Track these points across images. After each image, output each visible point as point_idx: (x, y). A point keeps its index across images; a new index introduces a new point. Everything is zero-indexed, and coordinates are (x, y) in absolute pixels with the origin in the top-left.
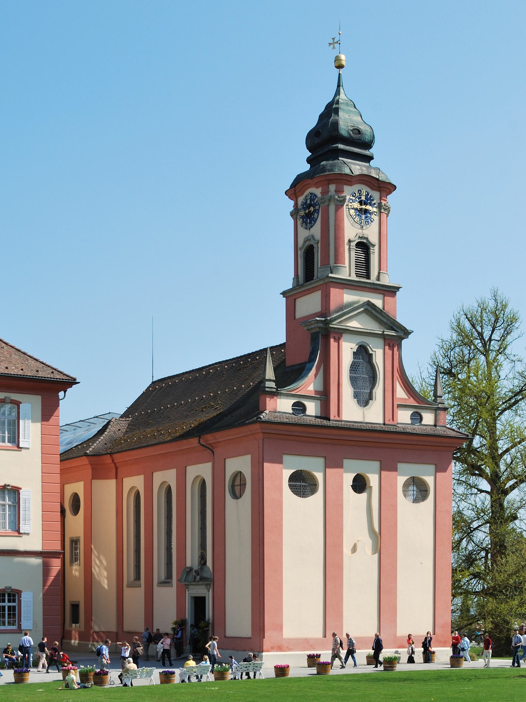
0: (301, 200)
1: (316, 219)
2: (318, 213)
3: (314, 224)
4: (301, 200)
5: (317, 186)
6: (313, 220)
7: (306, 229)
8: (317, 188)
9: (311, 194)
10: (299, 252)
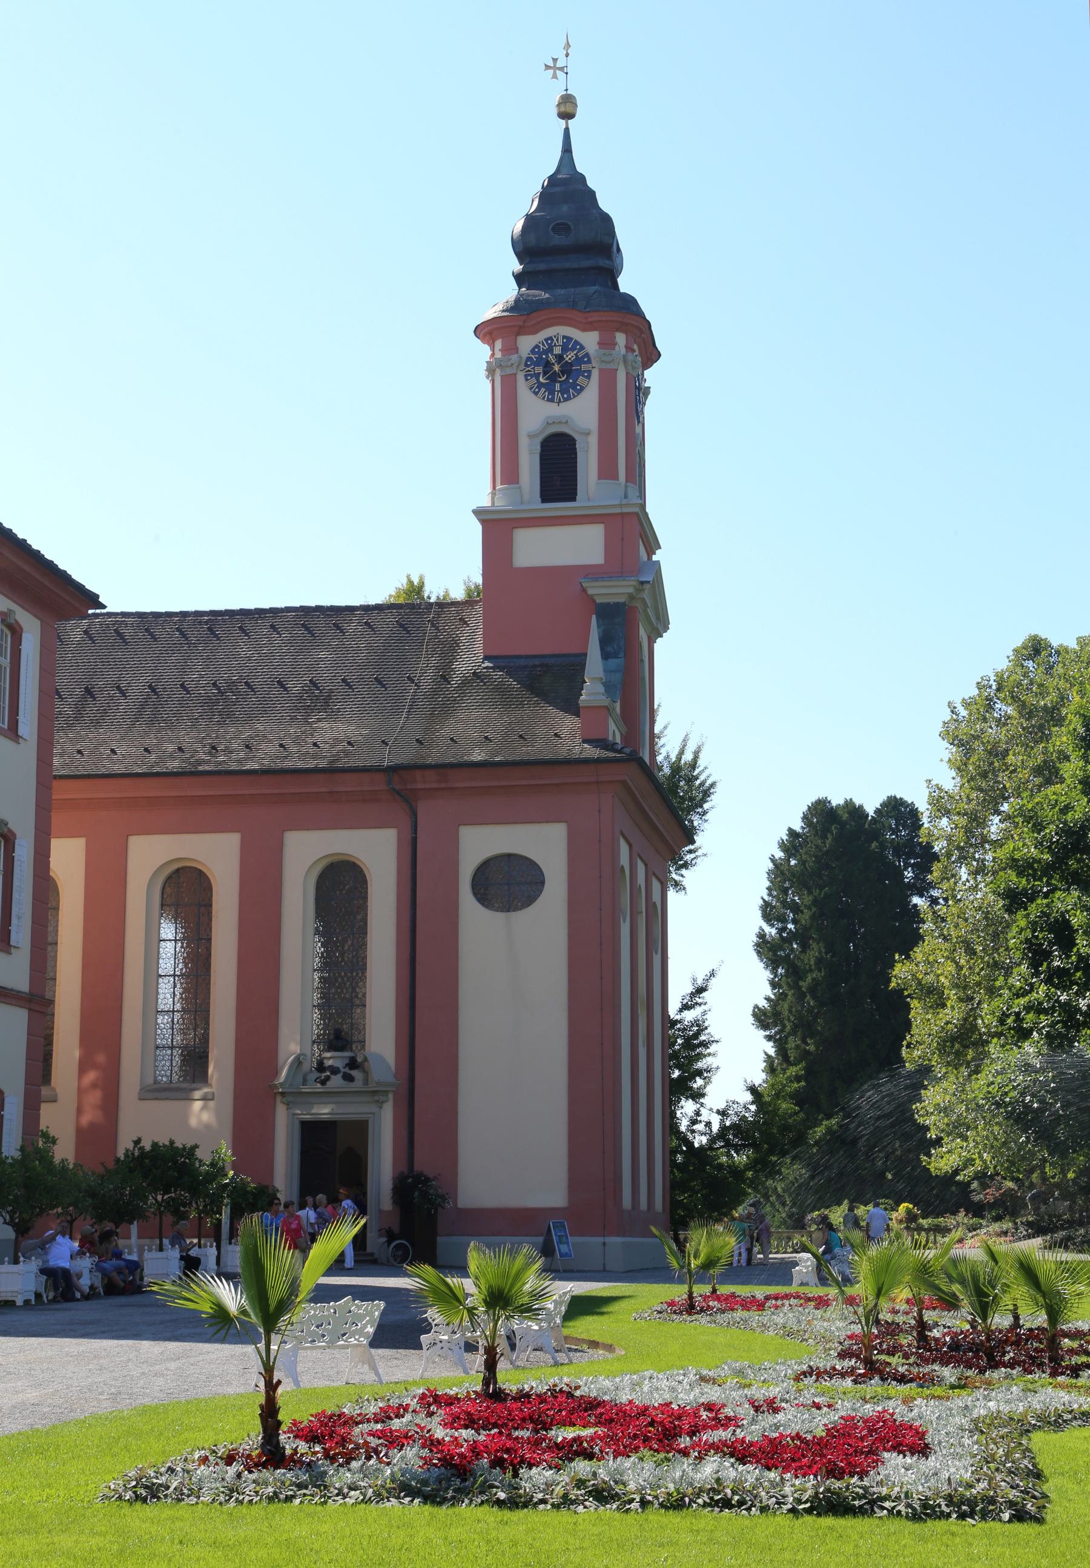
0: (527, 343)
1: (582, 389)
2: (589, 377)
3: (574, 396)
4: (527, 343)
5: (586, 327)
6: (575, 389)
7: (551, 400)
8: (584, 330)
9: (569, 339)
10: (524, 443)
